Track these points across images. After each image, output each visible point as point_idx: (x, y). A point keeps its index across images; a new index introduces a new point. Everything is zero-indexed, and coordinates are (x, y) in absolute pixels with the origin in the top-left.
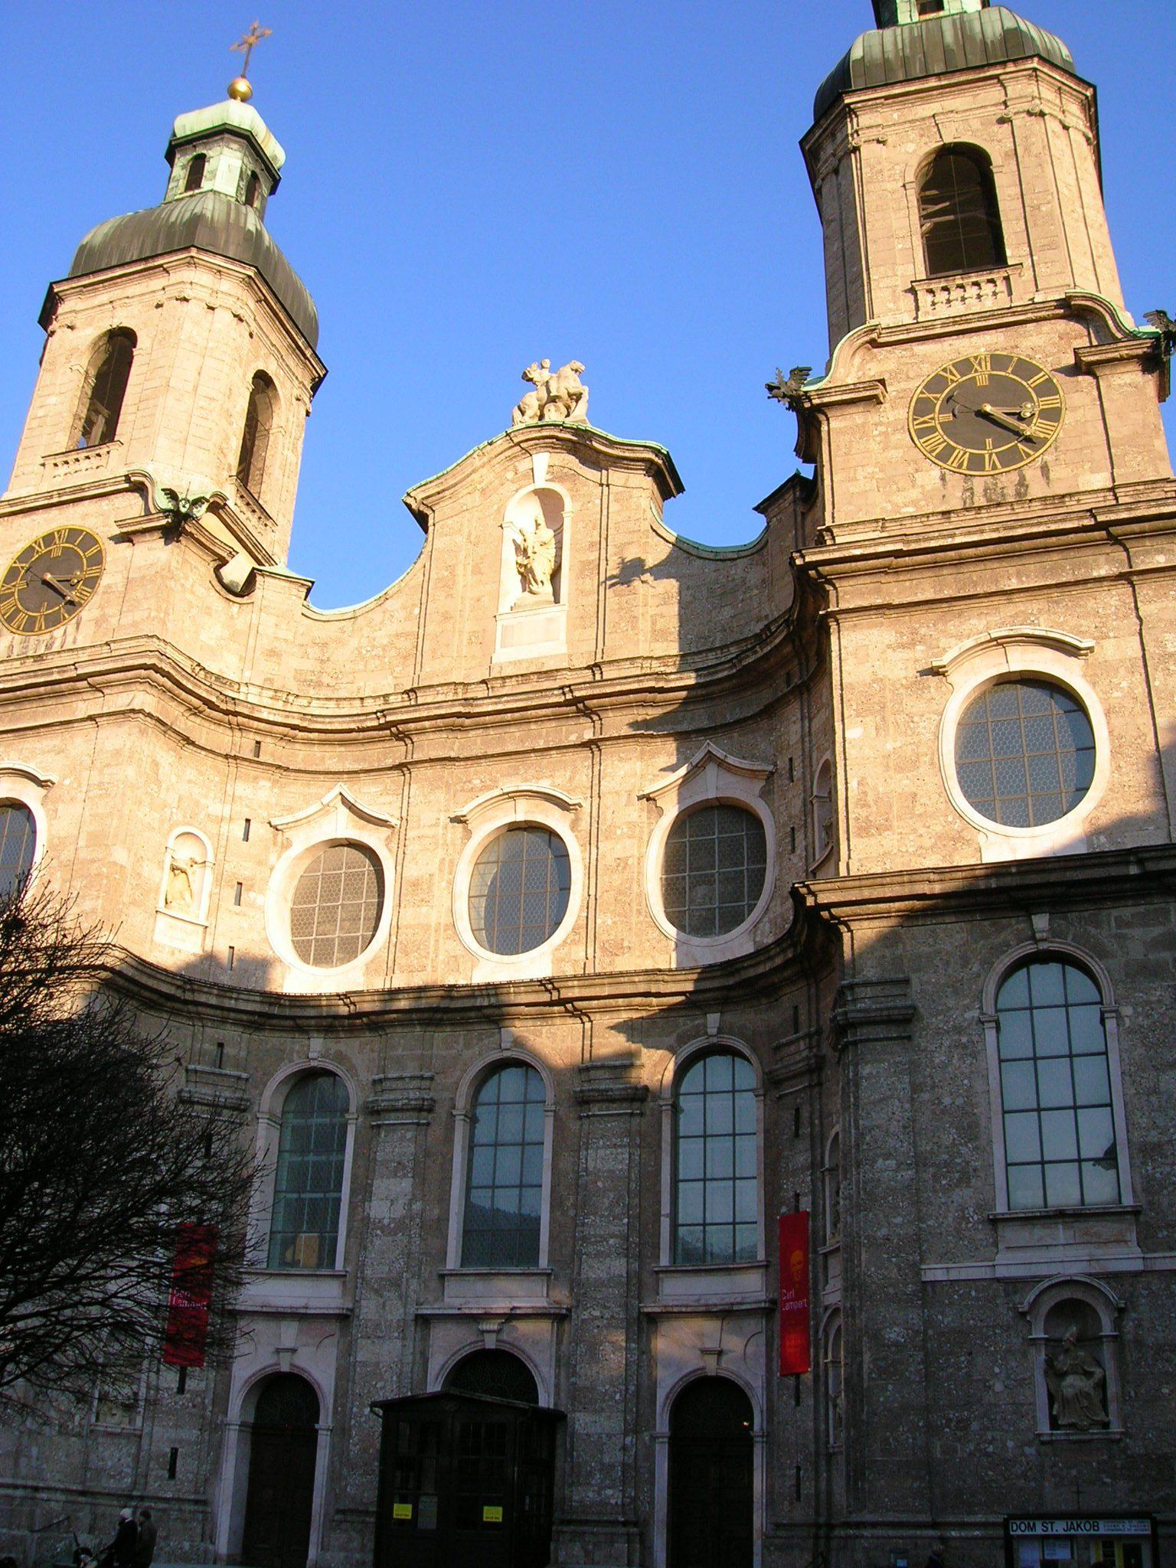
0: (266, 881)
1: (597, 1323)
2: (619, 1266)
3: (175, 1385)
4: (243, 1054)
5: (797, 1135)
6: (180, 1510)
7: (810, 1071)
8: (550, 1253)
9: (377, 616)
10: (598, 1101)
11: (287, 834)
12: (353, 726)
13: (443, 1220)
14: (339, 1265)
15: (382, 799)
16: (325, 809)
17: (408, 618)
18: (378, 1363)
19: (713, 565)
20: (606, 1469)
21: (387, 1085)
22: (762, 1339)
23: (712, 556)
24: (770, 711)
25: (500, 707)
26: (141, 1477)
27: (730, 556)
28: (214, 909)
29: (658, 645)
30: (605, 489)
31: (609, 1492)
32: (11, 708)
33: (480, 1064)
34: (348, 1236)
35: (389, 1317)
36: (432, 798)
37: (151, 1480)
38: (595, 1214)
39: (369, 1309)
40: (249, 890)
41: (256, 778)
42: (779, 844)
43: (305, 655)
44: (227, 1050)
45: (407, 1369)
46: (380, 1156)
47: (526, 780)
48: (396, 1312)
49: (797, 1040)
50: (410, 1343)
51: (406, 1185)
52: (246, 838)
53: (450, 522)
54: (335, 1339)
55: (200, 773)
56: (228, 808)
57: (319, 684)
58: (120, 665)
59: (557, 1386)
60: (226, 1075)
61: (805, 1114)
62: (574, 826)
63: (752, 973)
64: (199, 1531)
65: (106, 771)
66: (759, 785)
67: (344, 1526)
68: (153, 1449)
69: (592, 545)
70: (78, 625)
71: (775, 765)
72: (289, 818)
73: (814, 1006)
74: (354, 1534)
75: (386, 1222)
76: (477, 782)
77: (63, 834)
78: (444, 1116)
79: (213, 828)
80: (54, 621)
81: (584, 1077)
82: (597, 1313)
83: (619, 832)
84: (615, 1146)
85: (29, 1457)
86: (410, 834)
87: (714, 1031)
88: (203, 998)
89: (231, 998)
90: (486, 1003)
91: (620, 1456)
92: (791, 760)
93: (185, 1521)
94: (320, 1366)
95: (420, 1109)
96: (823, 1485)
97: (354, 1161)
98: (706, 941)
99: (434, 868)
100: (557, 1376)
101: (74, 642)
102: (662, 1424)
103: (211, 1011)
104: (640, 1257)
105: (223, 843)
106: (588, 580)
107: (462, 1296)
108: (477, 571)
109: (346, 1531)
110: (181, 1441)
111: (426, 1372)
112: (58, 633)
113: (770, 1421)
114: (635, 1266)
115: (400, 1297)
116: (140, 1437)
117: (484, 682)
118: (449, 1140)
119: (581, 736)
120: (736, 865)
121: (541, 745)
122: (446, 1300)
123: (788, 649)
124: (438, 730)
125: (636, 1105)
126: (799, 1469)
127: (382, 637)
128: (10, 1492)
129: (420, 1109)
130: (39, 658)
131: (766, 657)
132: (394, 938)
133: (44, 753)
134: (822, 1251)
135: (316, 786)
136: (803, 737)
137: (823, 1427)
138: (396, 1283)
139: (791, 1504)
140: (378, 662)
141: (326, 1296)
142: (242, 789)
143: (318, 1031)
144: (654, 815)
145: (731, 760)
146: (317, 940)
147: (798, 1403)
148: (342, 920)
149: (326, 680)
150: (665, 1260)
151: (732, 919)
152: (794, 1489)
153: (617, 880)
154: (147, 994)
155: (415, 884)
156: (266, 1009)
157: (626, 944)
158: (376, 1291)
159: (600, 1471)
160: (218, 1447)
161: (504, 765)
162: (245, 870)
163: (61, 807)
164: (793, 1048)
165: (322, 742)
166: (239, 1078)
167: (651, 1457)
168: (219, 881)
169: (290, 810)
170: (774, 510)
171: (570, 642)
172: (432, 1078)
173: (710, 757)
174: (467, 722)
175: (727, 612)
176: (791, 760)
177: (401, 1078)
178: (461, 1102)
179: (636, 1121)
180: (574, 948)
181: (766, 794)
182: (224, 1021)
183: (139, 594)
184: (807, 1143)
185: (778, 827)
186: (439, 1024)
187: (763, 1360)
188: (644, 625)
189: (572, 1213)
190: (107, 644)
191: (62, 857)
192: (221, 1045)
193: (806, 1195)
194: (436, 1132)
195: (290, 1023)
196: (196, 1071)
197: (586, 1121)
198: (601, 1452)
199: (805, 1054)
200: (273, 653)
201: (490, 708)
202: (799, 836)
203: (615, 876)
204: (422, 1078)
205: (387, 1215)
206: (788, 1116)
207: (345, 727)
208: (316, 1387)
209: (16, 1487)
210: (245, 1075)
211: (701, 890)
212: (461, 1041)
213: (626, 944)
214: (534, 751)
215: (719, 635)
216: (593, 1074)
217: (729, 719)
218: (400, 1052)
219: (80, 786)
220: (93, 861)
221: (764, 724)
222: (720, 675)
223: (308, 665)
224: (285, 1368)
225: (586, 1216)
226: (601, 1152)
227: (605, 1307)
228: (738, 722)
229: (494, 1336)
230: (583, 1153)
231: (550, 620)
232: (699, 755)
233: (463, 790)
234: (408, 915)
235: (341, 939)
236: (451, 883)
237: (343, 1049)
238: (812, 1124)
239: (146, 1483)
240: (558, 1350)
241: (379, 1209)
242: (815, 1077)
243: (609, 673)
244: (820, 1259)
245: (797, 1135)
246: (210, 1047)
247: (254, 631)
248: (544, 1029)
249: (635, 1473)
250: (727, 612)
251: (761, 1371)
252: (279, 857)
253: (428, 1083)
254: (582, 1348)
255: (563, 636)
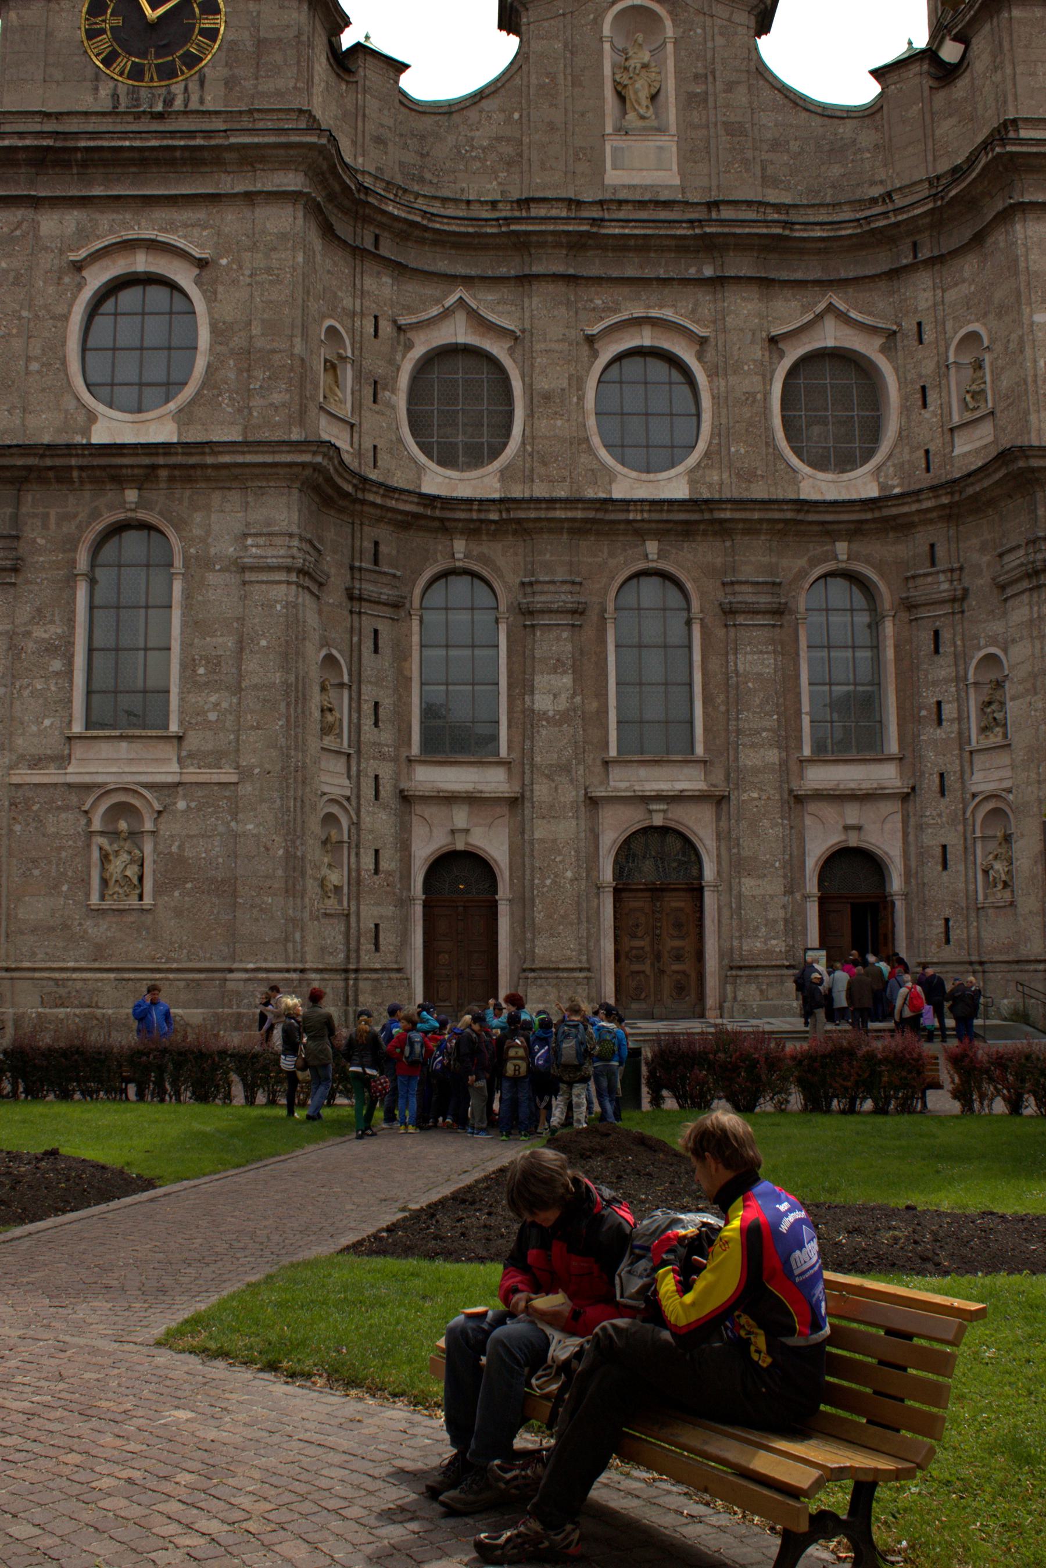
0: (395, 379)
1: (756, 803)
2: (773, 756)
3: (372, 867)
4: (394, 552)
5: (937, 651)
6: (390, 979)
7: (954, 600)
8: (705, 743)
9: (473, 115)
10: (744, 612)
11: (409, 335)
12: (471, 230)
13: (604, 710)
14: (503, 752)
15: (500, 308)
16: (447, 314)
17: (509, 120)
18: (554, 841)
19: (819, 119)
20: (770, 924)
21: (537, 588)
22: (898, 817)
23: (819, 110)
24: (894, 274)
25: (627, 231)
26: (352, 950)
27: (839, 114)
28: (357, 407)
29: (769, 191)
30: (708, 20)
31: (774, 942)
32: (134, 169)
33: (627, 573)
34: (509, 727)
35: (562, 799)
36: (556, 313)
37: (362, 953)
38: (748, 710)
39: (541, 791)
40: (384, 389)
41: (378, 273)
42: (905, 398)
43: (405, 146)
44: (383, 549)
45: (582, 844)
46: (538, 654)
47: (649, 307)
48: (569, 794)
49: (938, 573)
50: (582, 823)
51: (567, 680)
52: (376, 336)
53: (546, 24)
54: (506, 819)
55: (335, 264)
56: (358, 302)
57: (422, 180)
58: (283, 139)
59: (719, 856)
60: (385, 573)
61: (946, 635)
62: (700, 357)
63: (894, 511)
64: (406, 995)
65: (274, 255)
66: (878, 341)
67: (539, 982)
68: (362, 925)
69: (696, 76)
70: (202, 83)
71: (899, 325)
72: (413, 319)
73: (953, 546)
74: (549, 988)
75: (551, 713)
76: (599, 302)
77: (229, 319)
78: (595, 618)
79: (348, 322)
80: (168, 73)
81: (729, 589)
82: (755, 795)
83: (746, 368)
84: (761, 652)
85: (294, 942)
86: (539, 347)
87: (845, 557)
88: (371, 497)
89: (392, 498)
90: (639, 517)
91: (781, 914)
92: (919, 324)
93: (394, 988)
94: (493, 843)
95: (574, 612)
96: (973, 932)
97: (509, 657)
98: (830, 476)
99: (565, 385)
100: (718, 848)
101: (202, 101)
102: (812, 886)
103: (372, 510)
104: (787, 748)
105: (358, 338)
106: (695, 113)
107: (623, 781)
108: (576, 82)
109: (541, 986)
110: (381, 917)
111: (597, 848)
112: (177, 89)
113: (907, 882)
114: (784, 754)
115: (571, 781)
116: (348, 916)
117: (601, 203)
118: (603, 642)
119: (700, 270)
120: (846, 410)
121: (662, 273)
122: (612, 783)
123: (927, 220)
124: (558, 245)
125: (777, 617)
126: (947, 920)
127: (482, 136)
128: (287, 975)
129: (574, 612)
130: (160, 116)
131: (897, 224)
132: (529, 448)
133: (185, 225)
134: (968, 748)
135: (430, 290)
136: (935, 305)
137: (972, 887)
138: (566, 769)
139: (939, 947)
140: (478, 164)
141: (493, 781)
142: (369, 283)
143: (462, 533)
144: (775, 356)
145: (853, 314)
146: (439, 443)
147: (945, 867)
148: (465, 425)
149: (428, 176)
150: (807, 752)
151: (845, 461)
152: (942, 936)
153: (747, 412)
154: (330, 491)
155: (547, 397)
156: (420, 510)
157: (759, 472)
158: (548, 777)
159: (766, 925)
160: (406, 920)
161: (626, 290)
162: (381, 370)
163: (221, 289)
164: (929, 579)
165: (434, 243)
166: (394, 576)
167: (803, 913)
168: (358, 377)
169: (410, 310)
170: (893, 77)
171: (682, 174)
172: (581, 584)
173: (831, 308)
174: (590, 242)
175: (836, 170)
176: (919, 324)
177: (553, 582)
178: (611, 606)
179: (778, 630)
180: (707, 472)
181: (884, 350)
182: (380, 520)
183: (278, 58)
184: (951, 660)
185: (902, 382)
186: (588, 532)
187: (900, 835)
188: (758, 168)
189: (723, 708)
190: (250, 112)
191: (231, 345)
192: (376, 544)
193: (949, 702)
194: (589, 632)
195: (437, 524)
196: (360, 569)
197: (732, 630)
198: (766, 910)
199: (945, 586)
200: (379, 140)
201: (617, 231)
202: (932, 397)
203: (745, 409)
204: (573, 583)
205: (551, 707)
206: (926, 638)
207: (463, 229)
208: (492, 863)
209: (288, 971)
210: (399, 573)
211: (816, 430)
212: (606, 550)
213: (759, 472)
214: (658, 279)
215: (830, 192)
216: (737, 588)
217: (843, 275)
218: (548, 556)
219: (241, 267)
220: (274, 351)
221: (883, 284)
222: (843, 233)
223: (410, 158)
224: (460, 846)
225: (738, 712)
226: (749, 657)
227: (761, 790)
228: (856, 280)
229: (661, 815)
230: (731, 657)
231: (660, 148)
232: (821, 307)
233: (585, 309)
234: (543, 425)
235: (465, 444)
236: (581, 398)
237: (486, 551)
238: (955, 645)
239: (358, 957)
240: (717, 826)
241: (542, 702)
242: (956, 605)
243: (727, 213)
244: (966, 755)
245: (937, 651)
246: (368, 545)
247: (360, 114)
248: (686, 545)
249: (793, 926)
250: (836, 170)
251: (899, 844)
252: (404, 357)
253: (577, 588)
254: (744, 824)
255: (675, 167)
